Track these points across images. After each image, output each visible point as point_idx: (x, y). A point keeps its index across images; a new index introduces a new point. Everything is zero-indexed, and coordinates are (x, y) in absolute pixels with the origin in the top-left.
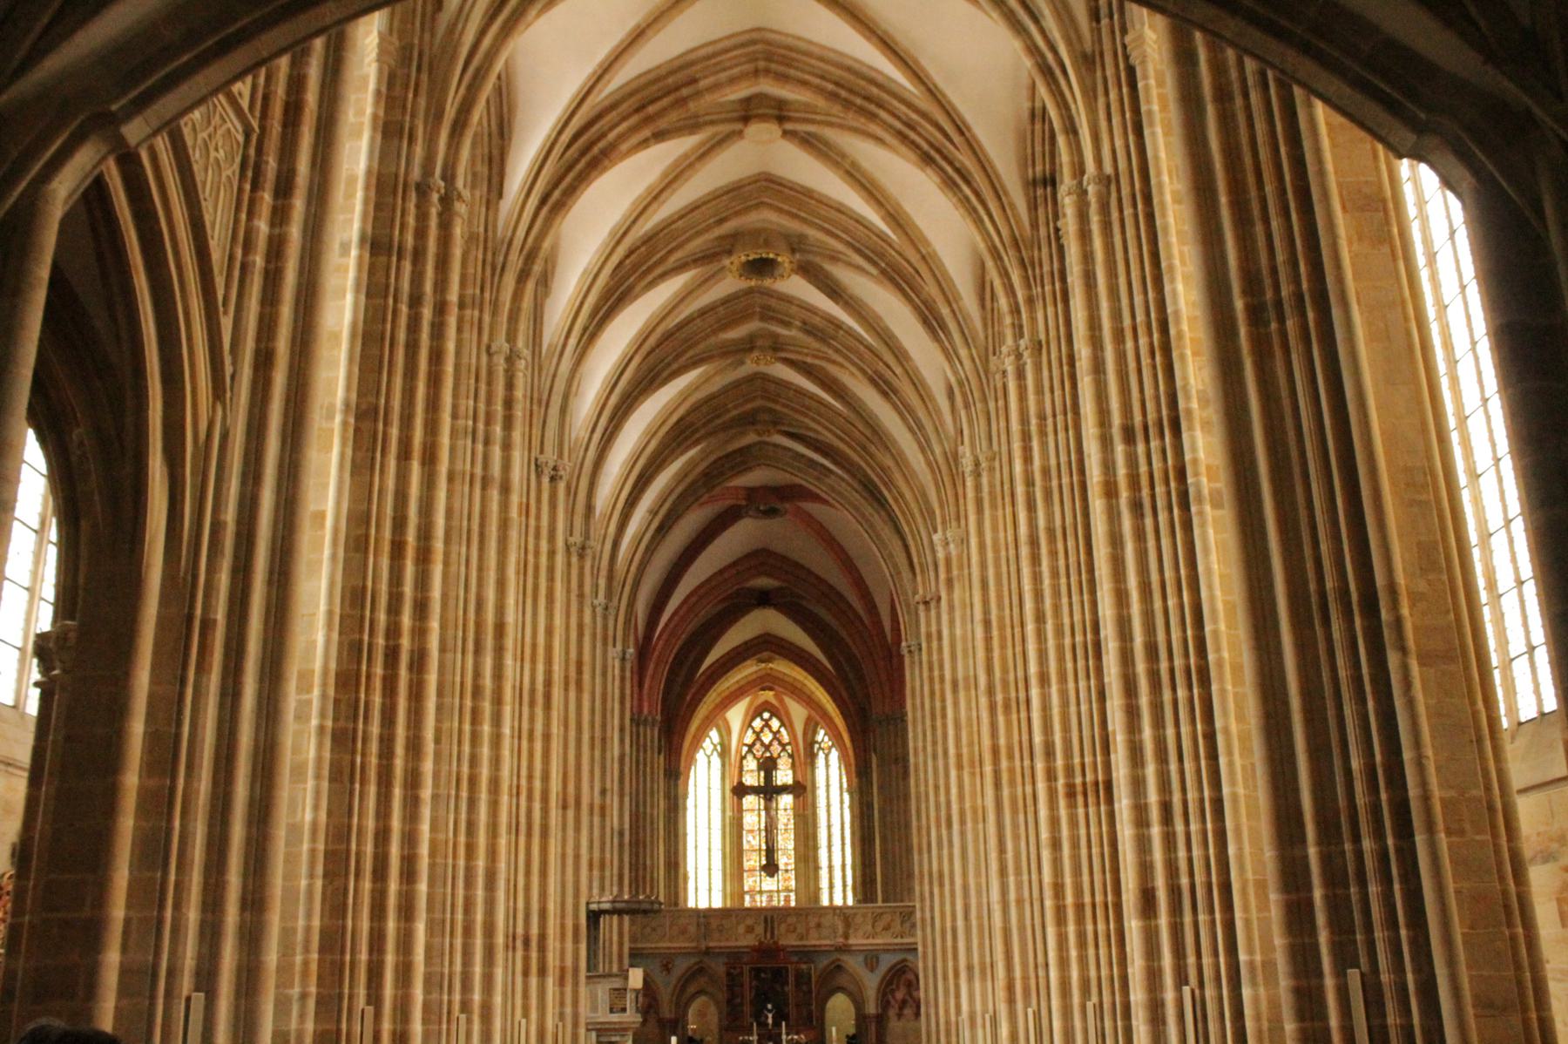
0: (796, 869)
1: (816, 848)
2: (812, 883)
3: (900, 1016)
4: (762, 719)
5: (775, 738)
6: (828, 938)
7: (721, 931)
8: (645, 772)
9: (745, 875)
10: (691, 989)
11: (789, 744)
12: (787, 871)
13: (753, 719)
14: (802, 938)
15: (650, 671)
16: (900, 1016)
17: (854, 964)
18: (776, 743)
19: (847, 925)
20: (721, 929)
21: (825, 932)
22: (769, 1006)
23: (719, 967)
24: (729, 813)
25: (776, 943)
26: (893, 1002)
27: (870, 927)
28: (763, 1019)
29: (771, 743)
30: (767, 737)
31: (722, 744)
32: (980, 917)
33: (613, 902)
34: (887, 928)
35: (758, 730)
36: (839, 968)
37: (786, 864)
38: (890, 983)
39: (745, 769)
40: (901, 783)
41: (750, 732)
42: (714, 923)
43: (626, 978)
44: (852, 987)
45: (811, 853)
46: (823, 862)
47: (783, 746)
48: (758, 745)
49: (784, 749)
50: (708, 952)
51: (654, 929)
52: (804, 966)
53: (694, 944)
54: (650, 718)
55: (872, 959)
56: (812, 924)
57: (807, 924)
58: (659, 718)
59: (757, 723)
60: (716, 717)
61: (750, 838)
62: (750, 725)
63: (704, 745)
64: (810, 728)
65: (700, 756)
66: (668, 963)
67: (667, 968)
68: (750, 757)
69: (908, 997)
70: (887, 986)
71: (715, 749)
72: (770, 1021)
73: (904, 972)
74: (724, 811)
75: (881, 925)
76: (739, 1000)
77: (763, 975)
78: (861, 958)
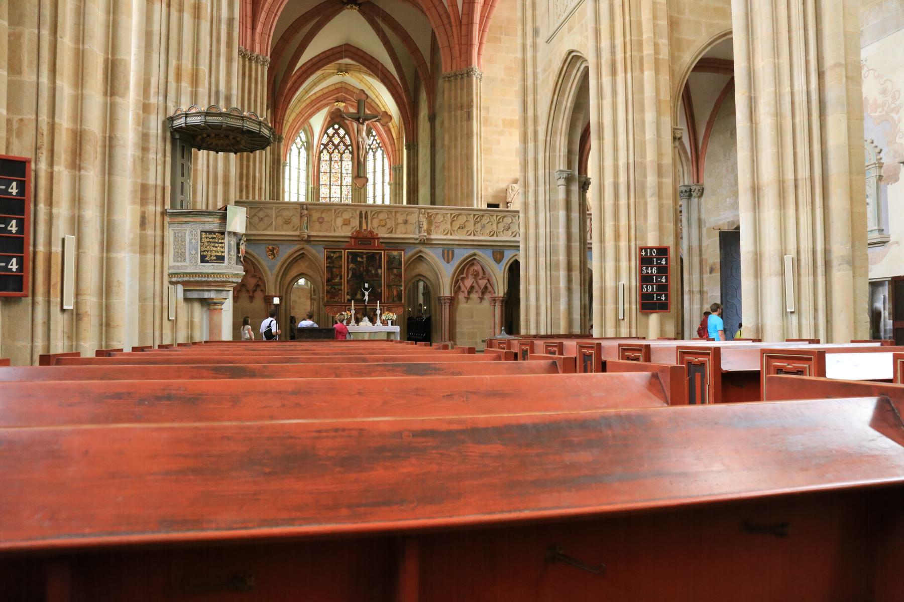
3: (468, 299)
4: (334, 129)
5: (341, 141)
6: (414, 233)
7: (321, 223)
8: (256, 101)
10: (294, 272)
11: (349, 145)
13: (328, 128)
14: (391, 232)
15: (262, 17)
16: (468, 299)
17: (433, 255)
18: (342, 144)
19: (430, 223)
20: (321, 221)
21: (410, 228)
22: (366, 285)
23: (320, 255)
24: (311, 186)
25: (371, 232)
26: (463, 288)
27: (449, 226)
28: (359, 296)
30: (336, 140)
32: (778, 114)
33: (207, 114)
34: (461, 228)
35: (331, 135)
36: (420, 258)
38: (462, 272)
39: (322, 159)
40: (465, 123)
41: (326, 135)
42: (316, 215)
43: (224, 217)
44: (429, 274)
47: (347, 146)
48: (330, 145)
49: (347, 148)
50: (308, 241)
51: (261, 220)
52: (395, 253)
53: (297, 233)
54: (261, 57)
55: (448, 251)
56: (400, 220)
57: (396, 219)
58: (268, 58)
60: (304, 122)
62: (326, 132)
63: (296, 141)
65: (294, 149)
66: (274, 249)
67: (272, 252)
68: (325, 152)
70: (458, 275)
72: (366, 298)
73: (473, 264)
74: (308, 185)
75: (457, 224)
76: (337, 280)
77: (359, 259)
78: (440, 251)
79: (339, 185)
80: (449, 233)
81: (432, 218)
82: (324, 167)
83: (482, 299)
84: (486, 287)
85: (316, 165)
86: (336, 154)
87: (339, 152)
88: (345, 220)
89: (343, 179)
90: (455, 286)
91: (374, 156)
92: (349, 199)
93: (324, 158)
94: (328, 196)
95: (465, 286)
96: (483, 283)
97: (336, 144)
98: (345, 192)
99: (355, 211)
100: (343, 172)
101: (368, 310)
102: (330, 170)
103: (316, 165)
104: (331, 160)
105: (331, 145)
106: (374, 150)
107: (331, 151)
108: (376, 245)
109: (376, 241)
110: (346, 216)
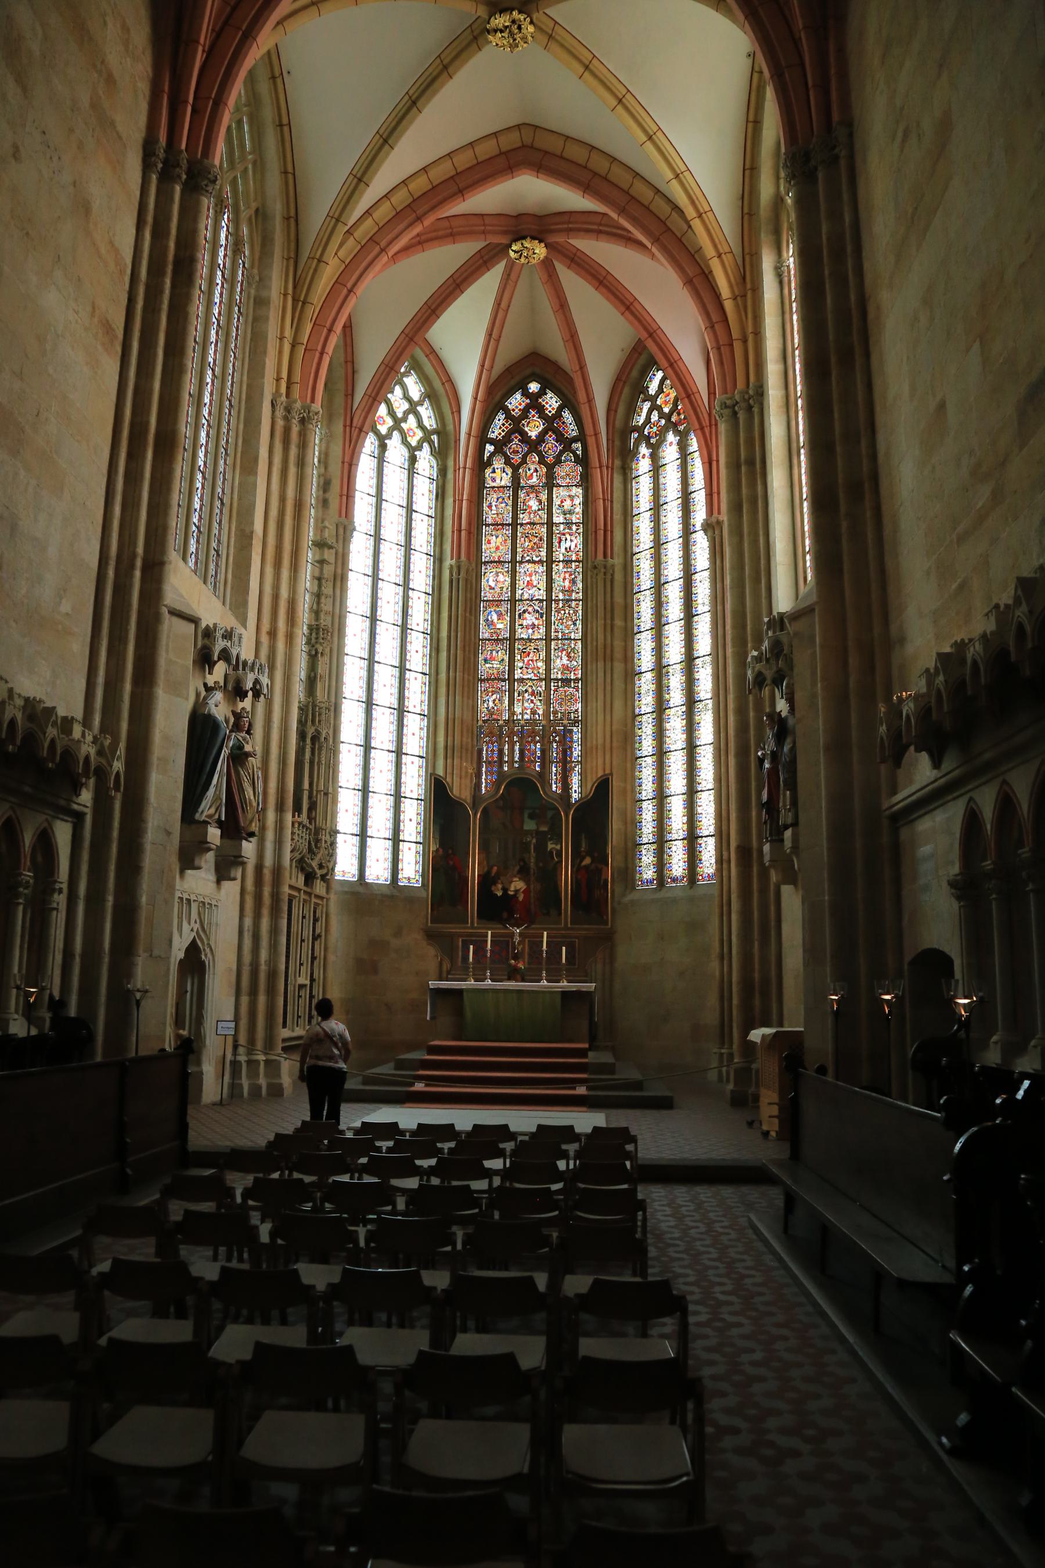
0: (584, 679)
1: (630, 633)
2: (618, 704)
4: (526, 394)
9: (481, 687)
11: (575, 440)
12: (566, 682)
13: (510, 394)
18: (550, 438)
29: (541, 437)
30: (534, 428)
35: (516, 413)
37: (566, 668)
39: (490, 483)
45: (618, 644)
46: (646, 660)
47: (567, 444)
48: (516, 442)
59: (516, 402)
61: (495, 617)
65: (396, 452)
68: (498, 463)
71: (427, 438)
79: (541, 562)
82: (496, 508)
85: (465, 497)
86: (532, 467)
89: (556, 544)
91: (654, 457)
92: (573, 604)
93: (494, 480)
94: (507, 596)
97: (534, 437)
98: (561, 580)
100: (556, 520)
102: (515, 517)
103: (465, 497)
104: (516, 485)
105: (516, 441)
106: (653, 441)
107: (517, 459)
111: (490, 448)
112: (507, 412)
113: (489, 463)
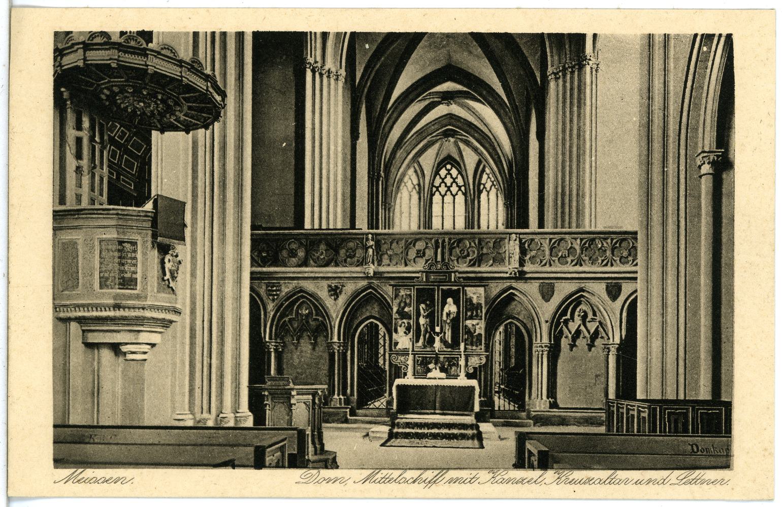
3: (572, 346)
4: (446, 169)
5: (454, 182)
14: (473, 265)
18: (454, 185)
19: (523, 252)
29: (452, 184)
30: (449, 181)
31: (419, 185)
47: (460, 187)
49: (460, 189)
59: (443, 172)
62: (437, 173)
64: (479, 171)
68: (437, 193)
69: (582, 328)
73: (579, 303)
80: (548, 264)
81: (526, 245)
82: (436, 209)
83: (591, 346)
84: (596, 332)
87: (452, 194)
88: (418, 251)
90: (555, 331)
95: (568, 329)
96: (592, 327)
99: (431, 239)
101: (441, 359)
108: (453, 280)
109: (453, 274)
110: (420, 245)
111: (434, 189)
112: (440, 176)
113: (434, 194)
